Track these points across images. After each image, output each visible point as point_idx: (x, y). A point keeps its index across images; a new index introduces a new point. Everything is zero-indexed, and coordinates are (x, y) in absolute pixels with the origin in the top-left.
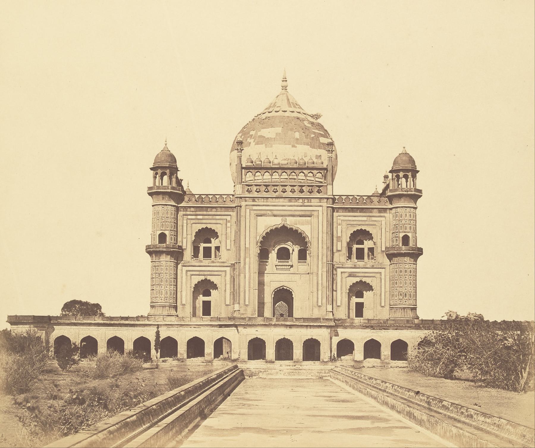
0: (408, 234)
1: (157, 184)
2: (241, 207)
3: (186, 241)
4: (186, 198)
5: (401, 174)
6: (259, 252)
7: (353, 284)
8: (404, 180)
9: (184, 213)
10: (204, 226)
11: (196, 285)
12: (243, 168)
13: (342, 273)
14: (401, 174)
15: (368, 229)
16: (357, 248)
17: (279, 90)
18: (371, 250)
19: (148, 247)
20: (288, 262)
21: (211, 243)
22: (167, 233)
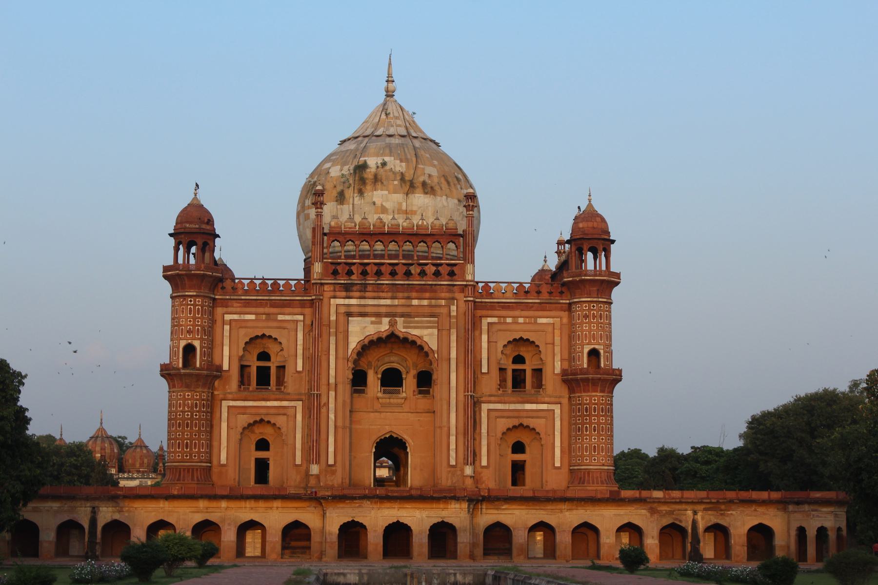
0: (597, 347)
1: (180, 261)
4: (228, 284)
6: (351, 377)
8: (590, 256)
9: (225, 310)
12: (325, 234)
13: (489, 411)
17: (381, 97)
18: (538, 372)
22: (197, 344)
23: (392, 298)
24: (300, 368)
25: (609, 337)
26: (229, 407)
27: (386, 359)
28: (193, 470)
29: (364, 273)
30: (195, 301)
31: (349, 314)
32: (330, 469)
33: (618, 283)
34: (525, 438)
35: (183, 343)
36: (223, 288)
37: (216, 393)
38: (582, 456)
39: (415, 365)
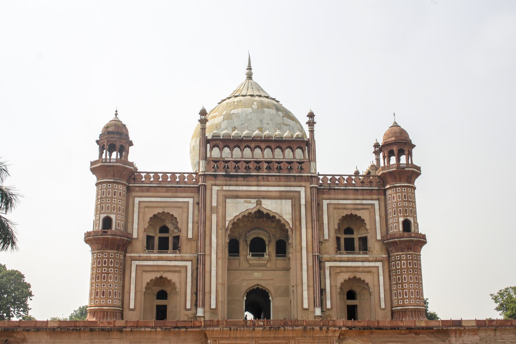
0: (408, 218)
2: (205, 186)
3: (137, 230)
5: (395, 149)
7: (345, 281)
10: (160, 211)
11: (148, 284)
12: (208, 141)
14: (395, 149)
15: (359, 213)
16: (345, 239)
18: (364, 241)
19: (88, 234)
20: (263, 256)
21: (168, 232)
22: (113, 216)
23: (258, 186)
24: (190, 236)
25: (415, 213)
26: (137, 265)
27: (254, 231)
28: (107, 312)
29: (237, 169)
30: (112, 186)
31: (226, 197)
32: (214, 311)
33: (419, 174)
34: (356, 289)
35: (103, 216)
36: (134, 179)
37: (128, 255)
38: (403, 299)
39: (274, 236)
